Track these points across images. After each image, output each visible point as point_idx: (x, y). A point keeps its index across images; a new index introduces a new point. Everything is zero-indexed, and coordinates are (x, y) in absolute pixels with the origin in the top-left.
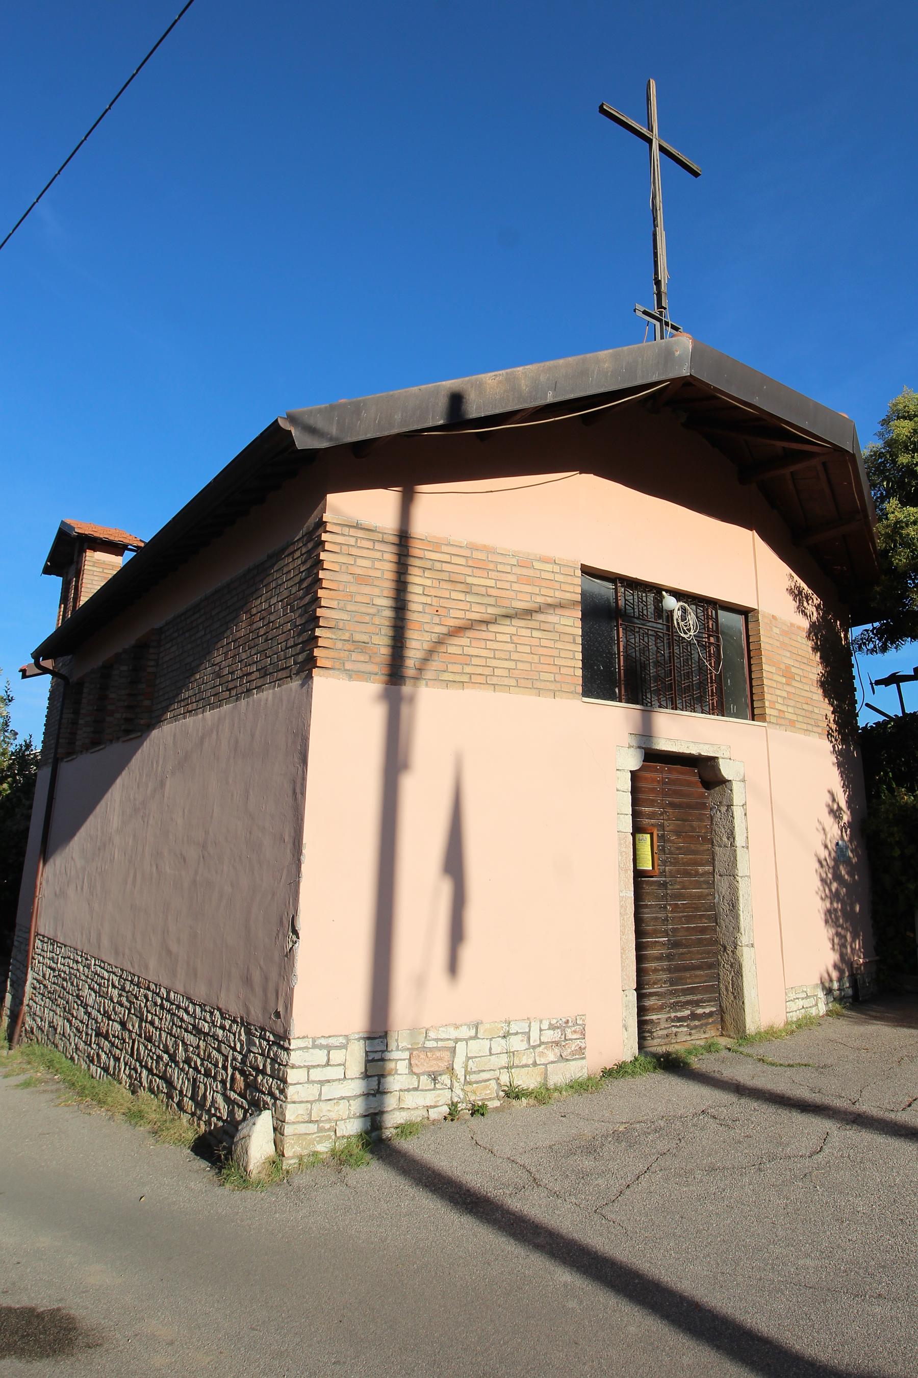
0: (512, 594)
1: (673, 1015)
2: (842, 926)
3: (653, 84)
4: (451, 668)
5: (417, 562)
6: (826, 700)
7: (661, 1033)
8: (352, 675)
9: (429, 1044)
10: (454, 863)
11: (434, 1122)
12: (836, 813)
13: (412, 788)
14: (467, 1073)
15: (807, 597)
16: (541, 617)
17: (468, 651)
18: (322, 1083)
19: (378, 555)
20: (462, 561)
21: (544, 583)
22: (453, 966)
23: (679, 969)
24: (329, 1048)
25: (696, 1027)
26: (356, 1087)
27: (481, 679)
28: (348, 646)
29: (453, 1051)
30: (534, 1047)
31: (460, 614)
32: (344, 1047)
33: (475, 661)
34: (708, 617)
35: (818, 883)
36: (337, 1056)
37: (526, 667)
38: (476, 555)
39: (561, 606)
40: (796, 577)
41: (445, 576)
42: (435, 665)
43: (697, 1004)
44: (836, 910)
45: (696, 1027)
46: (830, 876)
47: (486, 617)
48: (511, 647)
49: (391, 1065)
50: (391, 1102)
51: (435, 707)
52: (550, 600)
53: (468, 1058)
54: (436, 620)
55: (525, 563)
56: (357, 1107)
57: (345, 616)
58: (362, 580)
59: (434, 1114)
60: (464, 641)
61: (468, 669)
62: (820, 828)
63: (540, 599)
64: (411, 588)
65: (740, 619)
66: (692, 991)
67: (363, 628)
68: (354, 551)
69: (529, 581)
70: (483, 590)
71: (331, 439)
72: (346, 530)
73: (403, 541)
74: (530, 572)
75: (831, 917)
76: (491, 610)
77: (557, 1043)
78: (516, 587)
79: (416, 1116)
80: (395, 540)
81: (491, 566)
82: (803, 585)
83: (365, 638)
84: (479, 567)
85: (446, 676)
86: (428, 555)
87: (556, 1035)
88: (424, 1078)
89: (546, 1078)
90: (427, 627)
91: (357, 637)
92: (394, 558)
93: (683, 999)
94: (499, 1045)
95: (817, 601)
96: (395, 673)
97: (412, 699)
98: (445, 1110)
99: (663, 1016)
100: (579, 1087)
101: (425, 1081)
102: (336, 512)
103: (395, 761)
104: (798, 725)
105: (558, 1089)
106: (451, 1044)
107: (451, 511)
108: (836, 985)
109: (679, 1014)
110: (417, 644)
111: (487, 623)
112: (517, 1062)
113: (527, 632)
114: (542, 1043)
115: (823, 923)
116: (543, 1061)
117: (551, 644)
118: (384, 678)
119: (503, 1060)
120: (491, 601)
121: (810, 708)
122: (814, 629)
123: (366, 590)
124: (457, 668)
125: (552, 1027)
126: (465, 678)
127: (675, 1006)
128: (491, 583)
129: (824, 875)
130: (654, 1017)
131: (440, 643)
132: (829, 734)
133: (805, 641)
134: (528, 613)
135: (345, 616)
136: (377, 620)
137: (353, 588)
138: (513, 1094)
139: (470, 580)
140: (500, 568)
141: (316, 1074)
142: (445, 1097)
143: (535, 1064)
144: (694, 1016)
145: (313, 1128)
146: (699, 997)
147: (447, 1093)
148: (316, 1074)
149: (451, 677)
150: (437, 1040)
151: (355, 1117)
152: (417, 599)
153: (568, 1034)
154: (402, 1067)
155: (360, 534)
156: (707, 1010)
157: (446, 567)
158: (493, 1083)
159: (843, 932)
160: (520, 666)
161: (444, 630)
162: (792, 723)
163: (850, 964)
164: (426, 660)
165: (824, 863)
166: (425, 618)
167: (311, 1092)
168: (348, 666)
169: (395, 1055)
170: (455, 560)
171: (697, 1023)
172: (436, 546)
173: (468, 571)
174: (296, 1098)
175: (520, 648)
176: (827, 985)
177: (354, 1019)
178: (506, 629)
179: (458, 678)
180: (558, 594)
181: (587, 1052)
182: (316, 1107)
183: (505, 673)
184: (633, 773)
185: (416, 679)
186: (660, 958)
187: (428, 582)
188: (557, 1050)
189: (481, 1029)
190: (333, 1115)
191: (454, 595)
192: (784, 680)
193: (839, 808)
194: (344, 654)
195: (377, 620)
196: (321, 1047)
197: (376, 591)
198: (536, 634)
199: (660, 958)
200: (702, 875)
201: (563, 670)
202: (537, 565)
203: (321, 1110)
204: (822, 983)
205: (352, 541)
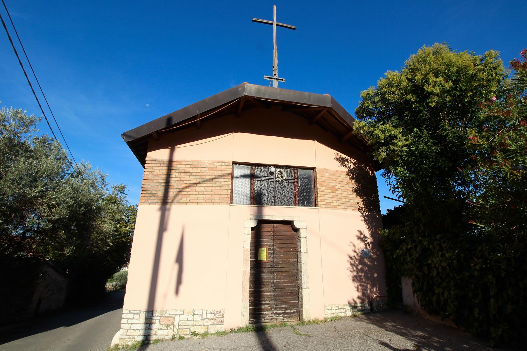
0: (206, 174)
1: (275, 312)
2: (364, 282)
3: (275, 7)
4: (183, 199)
5: (174, 168)
6: (359, 197)
7: (268, 318)
8: (150, 203)
9: (166, 315)
10: (180, 259)
11: (167, 340)
12: (363, 239)
13: (166, 236)
14: (179, 325)
15: (347, 161)
16: (216, 180)
17: (189, 193)
18: (132, 324)
19: (162, 168)
20: (189, 166)
21: (218, 169)
22: (177, 292)
23: (277, 296)
24: (134, 314)
25: (286, 317)
26: (142, 326)
27: (193, 201)
28: (150, 195)
29: (174, 318)
30: (204, 319)
31: (188, 182)
32: (139, 314)
33: (191, 196)
34: (295, 173)
35: (349, 266)
36: (137, 316)
37: (210, 196)
38: (194, 163)
39: (224, 176)
40: (340, 154)
41: (183, 171)
42: (178, 198)
43: (287, 309)
44: (360, 276)
45: (286, 317)
46: (357, 263)
47: (196, 182)
48: (205, 190)
49: (154, 321)
50: (153, 332)
51: (176, 211)
52: (220, 174)
53: (180, 321)
54: (179, 185)
55: (211, 164)
56: (142, 332)
57: (150, 187)
58: (156, 176)
59: (167, 338)
60: (188, 190)
61: (188, 199)
62: (351, 245)
63: (216, 174)
64: (172, 176)
65: (312, 171)
66: (285, 304)
67: (155, 189)
68: (154, 168)
69: (212, 169)
70: (196, 174)
71: (134, 138)
72: (152, 162)
73: (170, 163)
74: (213, 166)
75: (355, 279)
76: (198, 180)
77: (213, 319)
78: (207, 172)
79: (160, 338)
80: (167, 163)
81: (199, 166)
82: (342, 155)
83: (155, 192)
84: (196, 167)
85: (181, 201)
86: (178, 166)
87: (213, 316)
88: (164, 326)
89: (208, 330)
90: (175, 187)
91: (153, 192)
92: (167, 168)
93: (280, 306)
94: (191, 318)
95: (353, 161)
96: (165, 202)
97: (169, 209)
98: (171, 337)
99: (270, 312)
100: (218, 334)
101: (164, 327)
102: (149, 157)
103: (162, 228)
104: (338, 207)
105: (212, 334)
106: (174, 316)
107: (187, 153)
108: (359, 305)
109: (278, 312)
110: (172, 193)
111: (196, 184)
112: (197, 324)
113: (211, 185)
114: (207, 318)
115: (351, 281)
116: (207, 324)
117: (219, 188)
118: (161, 203)
119: (192, 323)
120: (199, 177)
121: (347, 200)
122: (351, 172)
123: (157, 178)
124: (185, 198)
125: (211, 313)
126: (188, 201)
127: (276, 309)
128: (199, 171)
129: (353, 263)
130: (266, 312)
131: (180, 191)
132: (359, 209)
133: (345, 176)
134: (211, 180)
135: (150, 187)
136: (159, 187)
137: (153, 179)
138: (195, 334)
139: (191, 171)
140: (202, 166)
141: (130, 321)
142: (171, 333)
143: (204, 325)
144: (285, 313)
145: (127, 337)
146: (289, 306)
147: (172, 331)
148: (130, 321)
149: (183, 201)
150: (169, 314)
151: (141, 335)
152: (173, 179)
153: (217, 316)
154: (157, 322)
155: (156, 162)
156: (292, 311)
157: (183, 168)
158: (188, 330)
159: (365, 284)
160: (207, 196)
161: (181, 187)
162: (335, 207)
163: (368, 297)
164: (175, 197)
165: (354, 258)
166: (176, 185)
167: (128, 326)
168: (149, 201)
169: (155, 318)
170: (186, 166)
171: (287, 315)
172: (181, 163)
173: (191, 169)
174: (123, 328)
175: (207, 190)
176: (353, 305)
177: (143, 305)
178: (204, 185)
179: (185, 202)
180: (223, 172)
181: (224, 323)
182: (129, 331)
183: (202, 199)
184: (253, 229)
185: (171, 203)
186: (270, 291)
187: (177, 174)
188: (213, 321)
189: (185, 312)
190: (134, 334)
191: (186, 177)
192: (331, 191)
193: (365, 237)
194: (148, 198)
195: (159, 187)
196: (132, 313)
197: (160, 178)
198: (213, 185)
199: (270, 291)
200: (292, 262)
201: (223, 196)
202: (215, 164)
203: (130, 332)
204: (349, 303)
205: (154, 165)
